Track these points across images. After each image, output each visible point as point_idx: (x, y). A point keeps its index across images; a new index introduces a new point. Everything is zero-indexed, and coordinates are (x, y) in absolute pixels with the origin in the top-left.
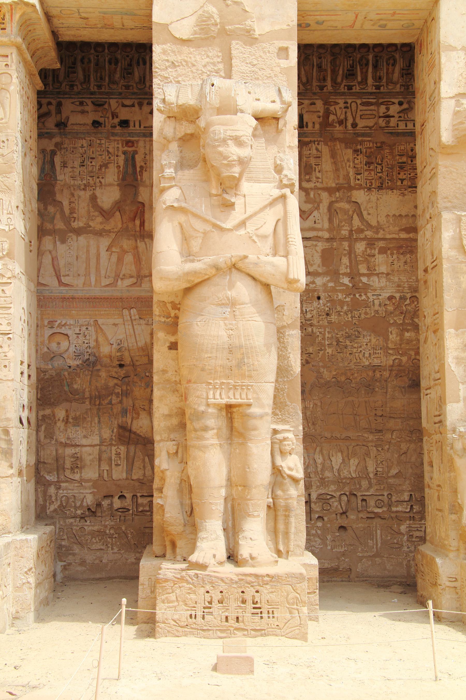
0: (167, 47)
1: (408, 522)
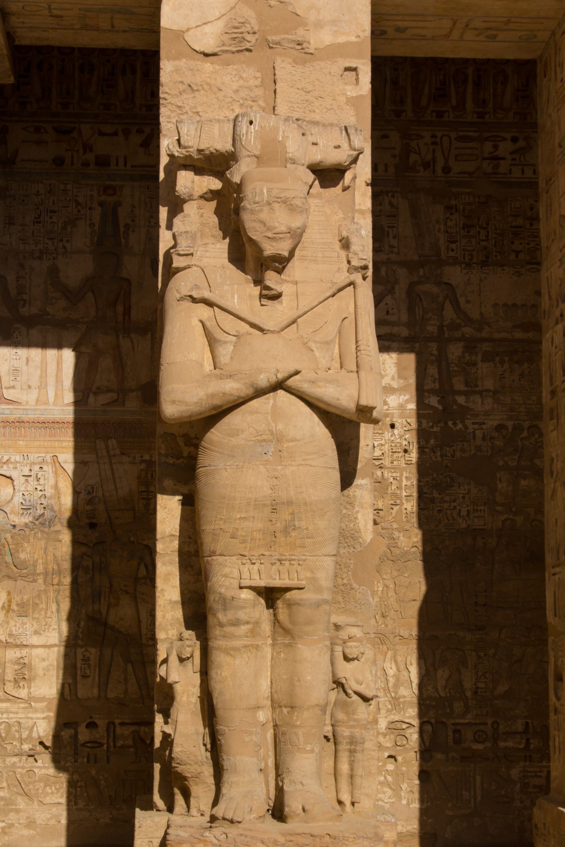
0: (182, 63)
1: (522, 764)
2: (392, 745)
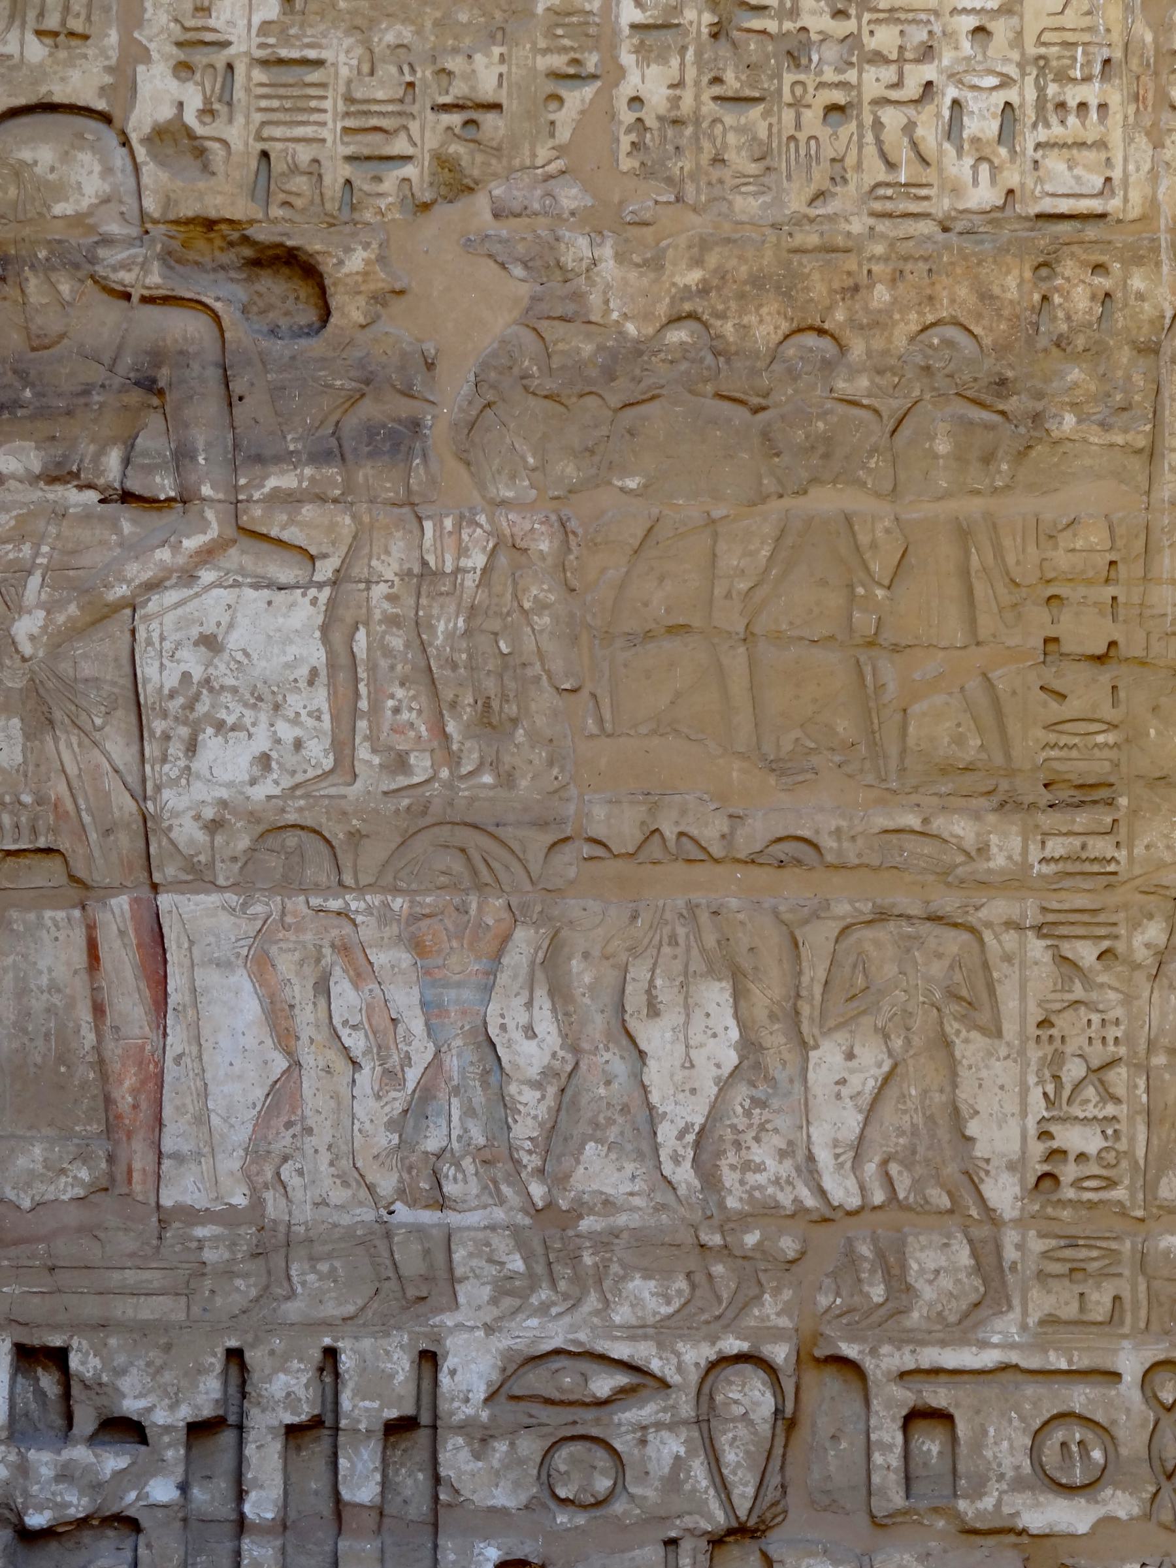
2: (523, 1498)
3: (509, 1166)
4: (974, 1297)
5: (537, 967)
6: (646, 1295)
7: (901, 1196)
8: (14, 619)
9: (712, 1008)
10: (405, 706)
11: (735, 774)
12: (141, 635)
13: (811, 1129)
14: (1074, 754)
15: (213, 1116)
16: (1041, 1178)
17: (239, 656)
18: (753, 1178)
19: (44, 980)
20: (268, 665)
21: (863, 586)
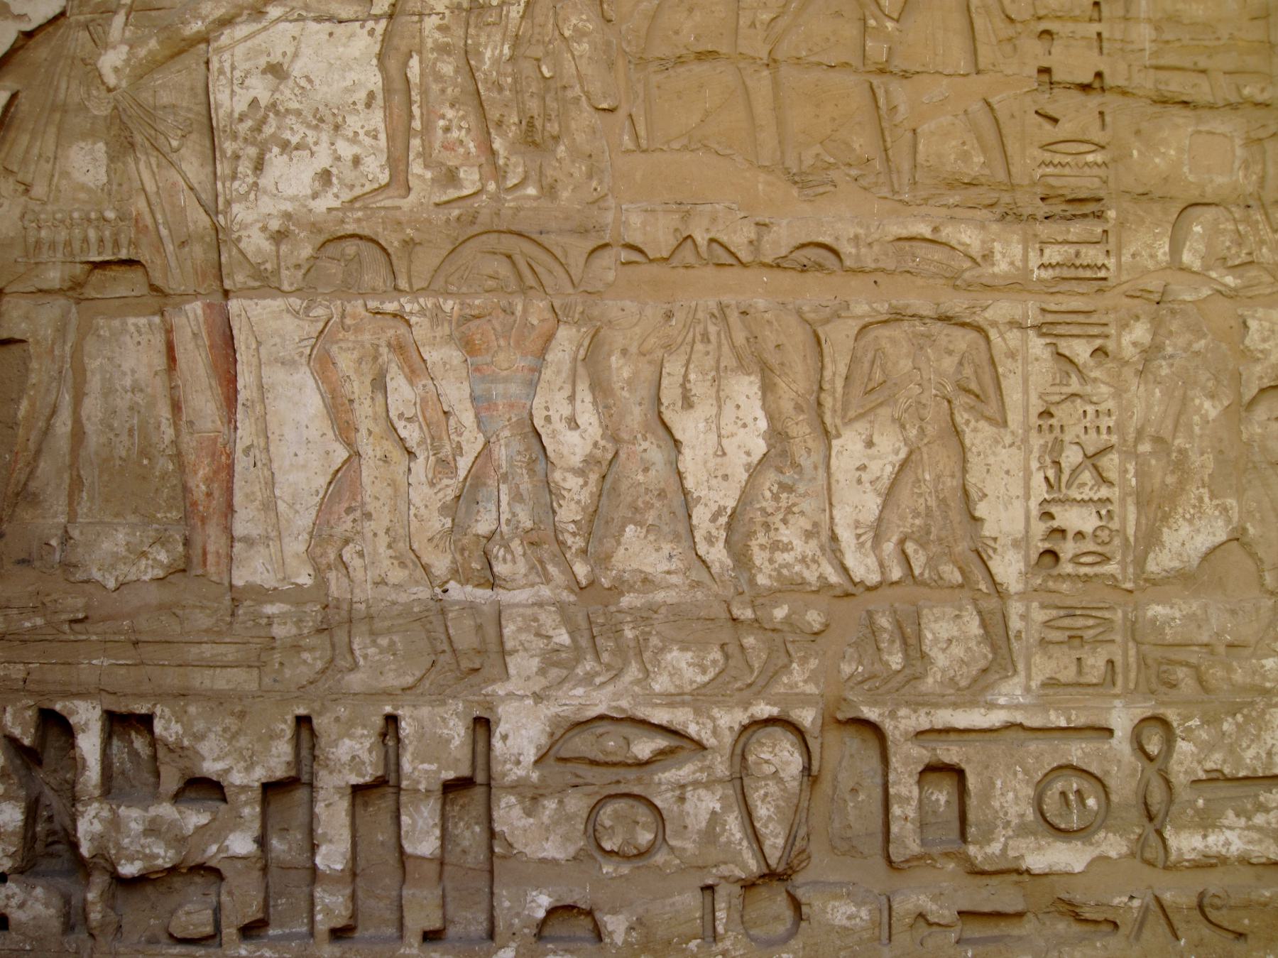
2: (572, 850)
3: (555, 548)
4: (982, 664)
5: (579, 364)
6: (683, 665)
7: (917, 572)
8: (100, 54)
9: (742, 400)
10: (456, 126)
11: (760, 187)
12: (215, 65)
13: (835, 512)
14: (1067, 171)
15: (280, 502)
16: (1041, 554)
17: (303, 83)
18: (782, 557)
19: (128, 382)
20: (328, 91)
21: (876, 19)
